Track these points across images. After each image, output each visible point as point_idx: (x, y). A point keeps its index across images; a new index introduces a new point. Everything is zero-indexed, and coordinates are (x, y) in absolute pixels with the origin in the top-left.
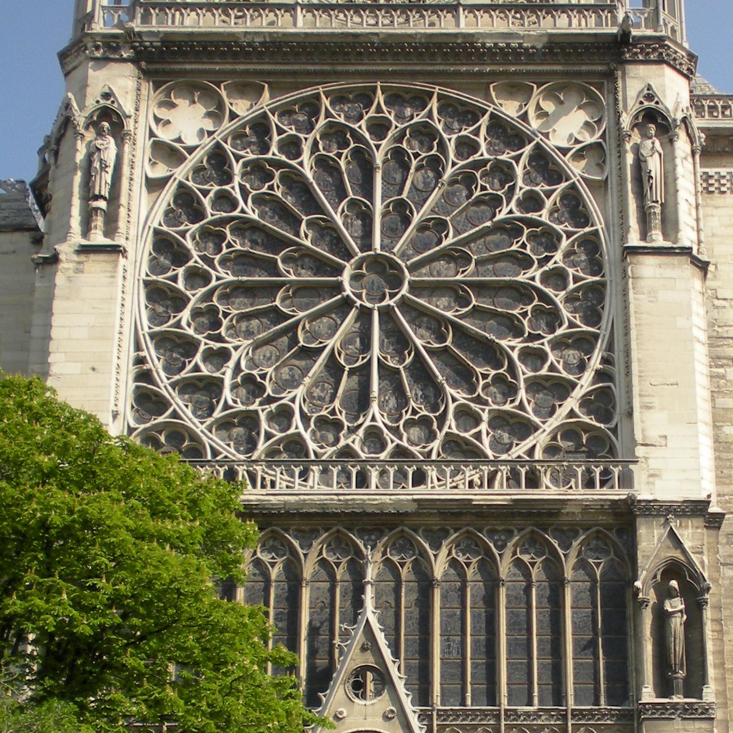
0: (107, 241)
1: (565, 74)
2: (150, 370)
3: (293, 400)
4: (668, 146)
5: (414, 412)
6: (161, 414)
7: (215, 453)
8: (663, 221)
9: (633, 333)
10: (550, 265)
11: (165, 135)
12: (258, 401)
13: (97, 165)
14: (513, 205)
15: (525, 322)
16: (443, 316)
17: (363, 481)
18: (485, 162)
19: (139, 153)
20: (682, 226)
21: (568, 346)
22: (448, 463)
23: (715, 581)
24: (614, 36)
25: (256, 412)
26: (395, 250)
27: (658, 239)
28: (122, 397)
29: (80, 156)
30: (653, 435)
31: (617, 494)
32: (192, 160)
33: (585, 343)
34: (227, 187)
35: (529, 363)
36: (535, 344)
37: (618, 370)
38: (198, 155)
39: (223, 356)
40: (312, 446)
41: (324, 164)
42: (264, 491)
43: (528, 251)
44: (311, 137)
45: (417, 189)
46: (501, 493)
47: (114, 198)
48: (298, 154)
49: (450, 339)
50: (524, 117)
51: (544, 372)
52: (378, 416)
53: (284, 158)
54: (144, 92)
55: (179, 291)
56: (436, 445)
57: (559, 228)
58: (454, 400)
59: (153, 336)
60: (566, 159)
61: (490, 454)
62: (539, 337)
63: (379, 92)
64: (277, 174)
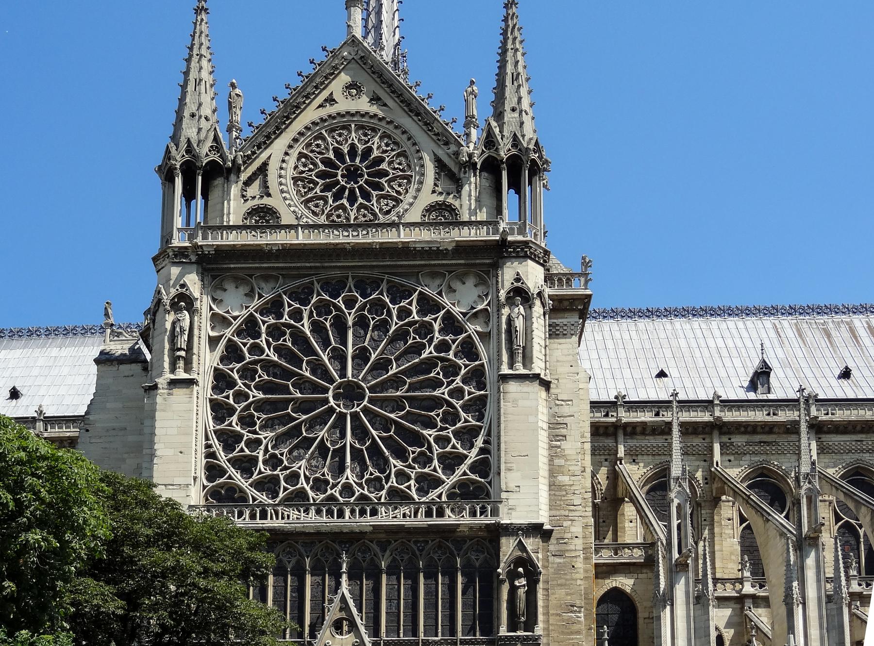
0: (185, 376)
1: (464, 265)
3: (300, 468)
4: (528, 310)
5: (371, 474)
7: (254, 499)
8: (524, 357)
9: (502, 426)
10: (454, 385)
13: (178, 329)
15: (438, 420)
16: (389, 417)
17: (341, 514)
18: (416, 322)
19: (204, 321)
20: (535, 360)
23: (544, 567)
25: (278, 475)
26: (360, 378)
28: (198, 468)
29: (168, 326)
32: (236, 324)
33: (473, 432)
36: (444, 433)
37: (493, 448)
38: (239, 321)
39: (258, 442)
40: (311, 494)
41: (317, 328)
42: (283, 521)
43: (441, 377)
45: (374, 340)
46: (421, 520)
48: (301, 319)
51: (448, 449)
53: (292, 322)
54: (206, 282)
55: (230, 404)
56: (384, 492)
57: (460, 362)
58: (395, 466)
59: (215, 432)
61: (415, 497)
62: (447, 428)
63: (350, 279)
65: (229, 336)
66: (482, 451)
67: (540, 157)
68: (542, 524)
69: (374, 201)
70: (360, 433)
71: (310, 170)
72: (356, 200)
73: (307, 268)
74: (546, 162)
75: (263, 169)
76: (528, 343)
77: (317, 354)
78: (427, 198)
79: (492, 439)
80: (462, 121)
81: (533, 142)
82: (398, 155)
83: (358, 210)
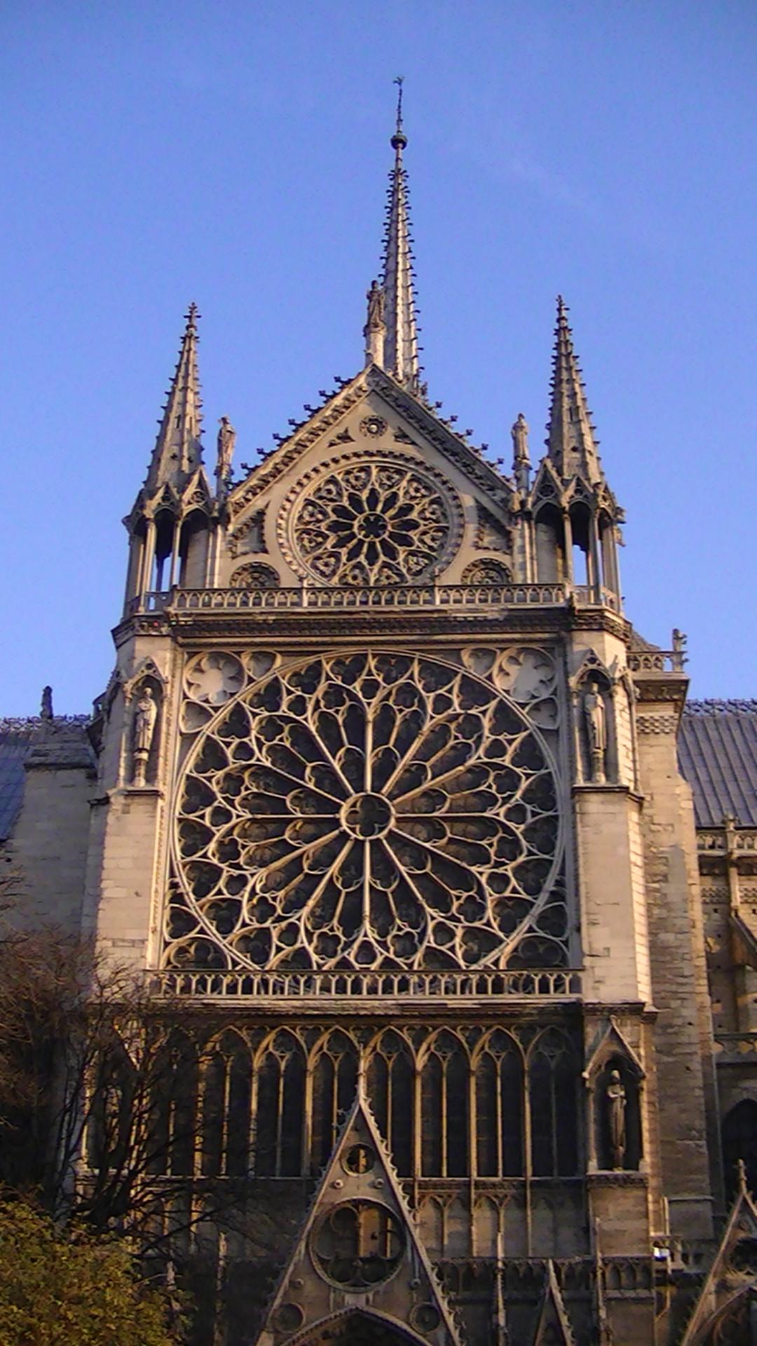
2: (181, 894)
5: (400, 929)
6: (191, 931)
7: (235, 964)
8: (605, 764)
11: (194, 697)
12: (270, 921)
13: (141, 723)
14: (481, 752)
20: (621, 768)
21: (528, 871)
22: (427, 973)
24: (562, 609)
25: (268, 929)
26: (384, 791)
27: (602, 780)
30: (599, 947)
31: (568, 997)
32: (219, 717)
34: (245, 740)
35: (495, 886)
36: (500, 870)
37: (569, 891)
39: (242, 880)
40: (315, 958)
41: (326, 722)
43: (493, 791)
44: (314, 697)
47: (154, 750)
48: (303, 711)
49: (429, 866)
50: (490, 678)
51: (507, 894)
52: (369, 932)
54: (179, 662)
56: (418, 957)
57: (518, 770)
58: (433, 918)
60: (524, 712)
61: (462, 963)
62: (504, 864)
64: (287, 728)
65: (208, 733)
66: (556, 896)
67: (612, 505)
68: (644, 1004)
69: (401, 557)
70: (384, 869)
71: (319, 521)
72: (377, 557)
73: (312, 644)
74: (619, 511)
75: (259, 519)
76: (611, 745)
77: (325, 759)
78: (468, 555)
79: (566, 879)
80: (510, 461)
81: (602, 487)
82: (432, 502)
83: (380, 571)
